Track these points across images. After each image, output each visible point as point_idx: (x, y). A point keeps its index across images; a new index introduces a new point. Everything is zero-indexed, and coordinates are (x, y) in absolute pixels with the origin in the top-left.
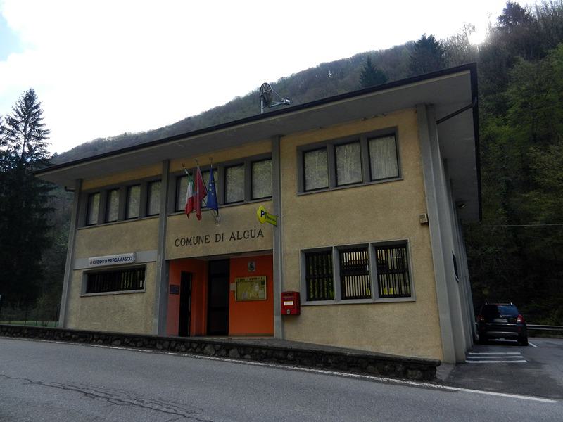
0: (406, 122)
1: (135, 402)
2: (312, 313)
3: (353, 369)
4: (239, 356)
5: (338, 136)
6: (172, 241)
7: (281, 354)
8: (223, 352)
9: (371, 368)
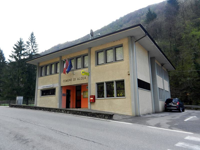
0: (125, 42)
1: (33, 123)
2: (98, 101)
3: (93, 116)
4: (69, 113)
5: (107, 47)
6: (62, 80)
7: (78, 113)
8: (66, 112)
9: (83, 114)
